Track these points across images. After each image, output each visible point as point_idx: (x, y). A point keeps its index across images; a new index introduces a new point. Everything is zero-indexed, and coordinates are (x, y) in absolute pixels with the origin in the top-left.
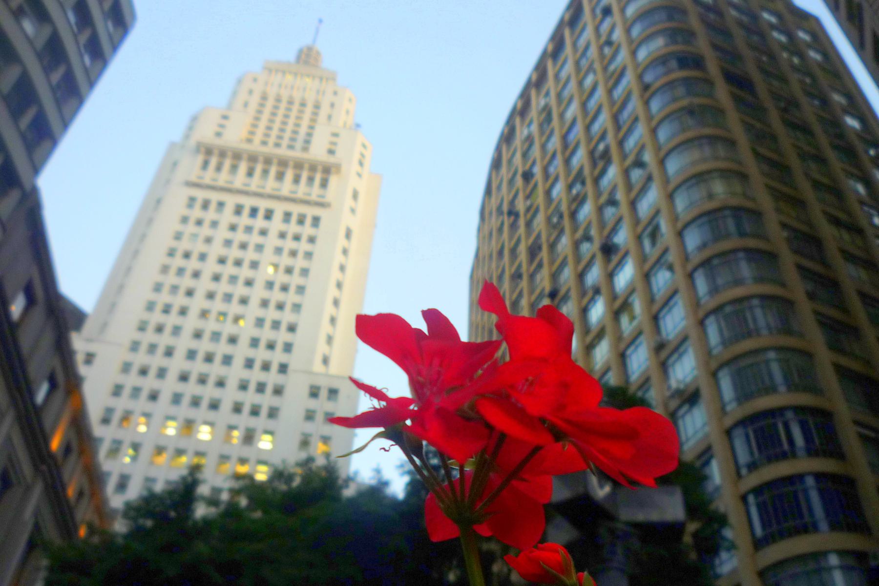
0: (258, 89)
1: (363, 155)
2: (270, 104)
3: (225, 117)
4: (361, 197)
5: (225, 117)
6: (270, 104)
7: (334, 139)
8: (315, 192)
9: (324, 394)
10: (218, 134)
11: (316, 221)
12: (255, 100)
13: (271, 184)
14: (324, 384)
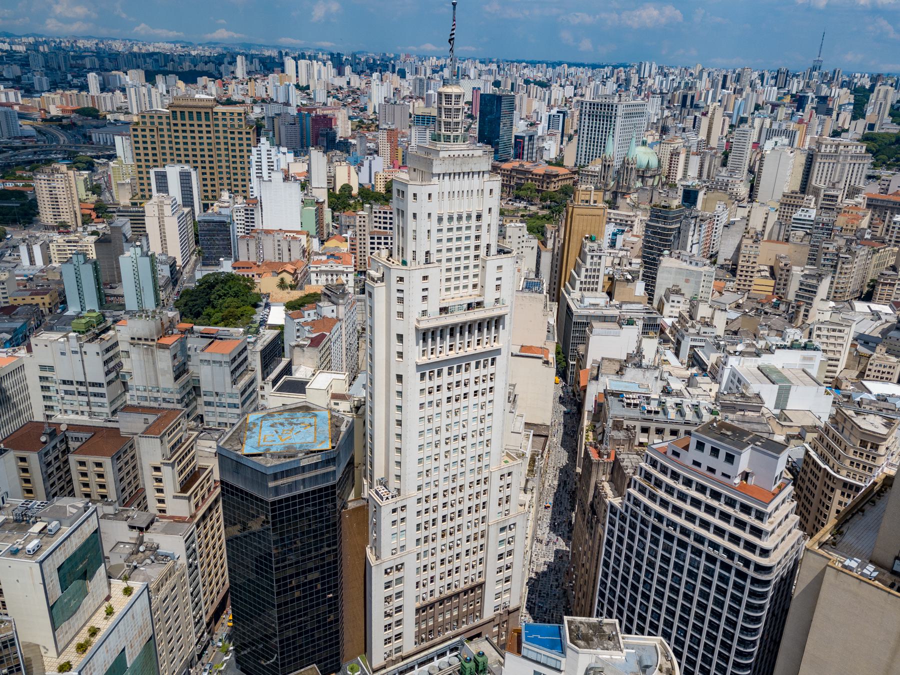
2: (445, 224)
3: (425, 278)
6: (445, 224)
11: (493, 360)
12: (435, 226)
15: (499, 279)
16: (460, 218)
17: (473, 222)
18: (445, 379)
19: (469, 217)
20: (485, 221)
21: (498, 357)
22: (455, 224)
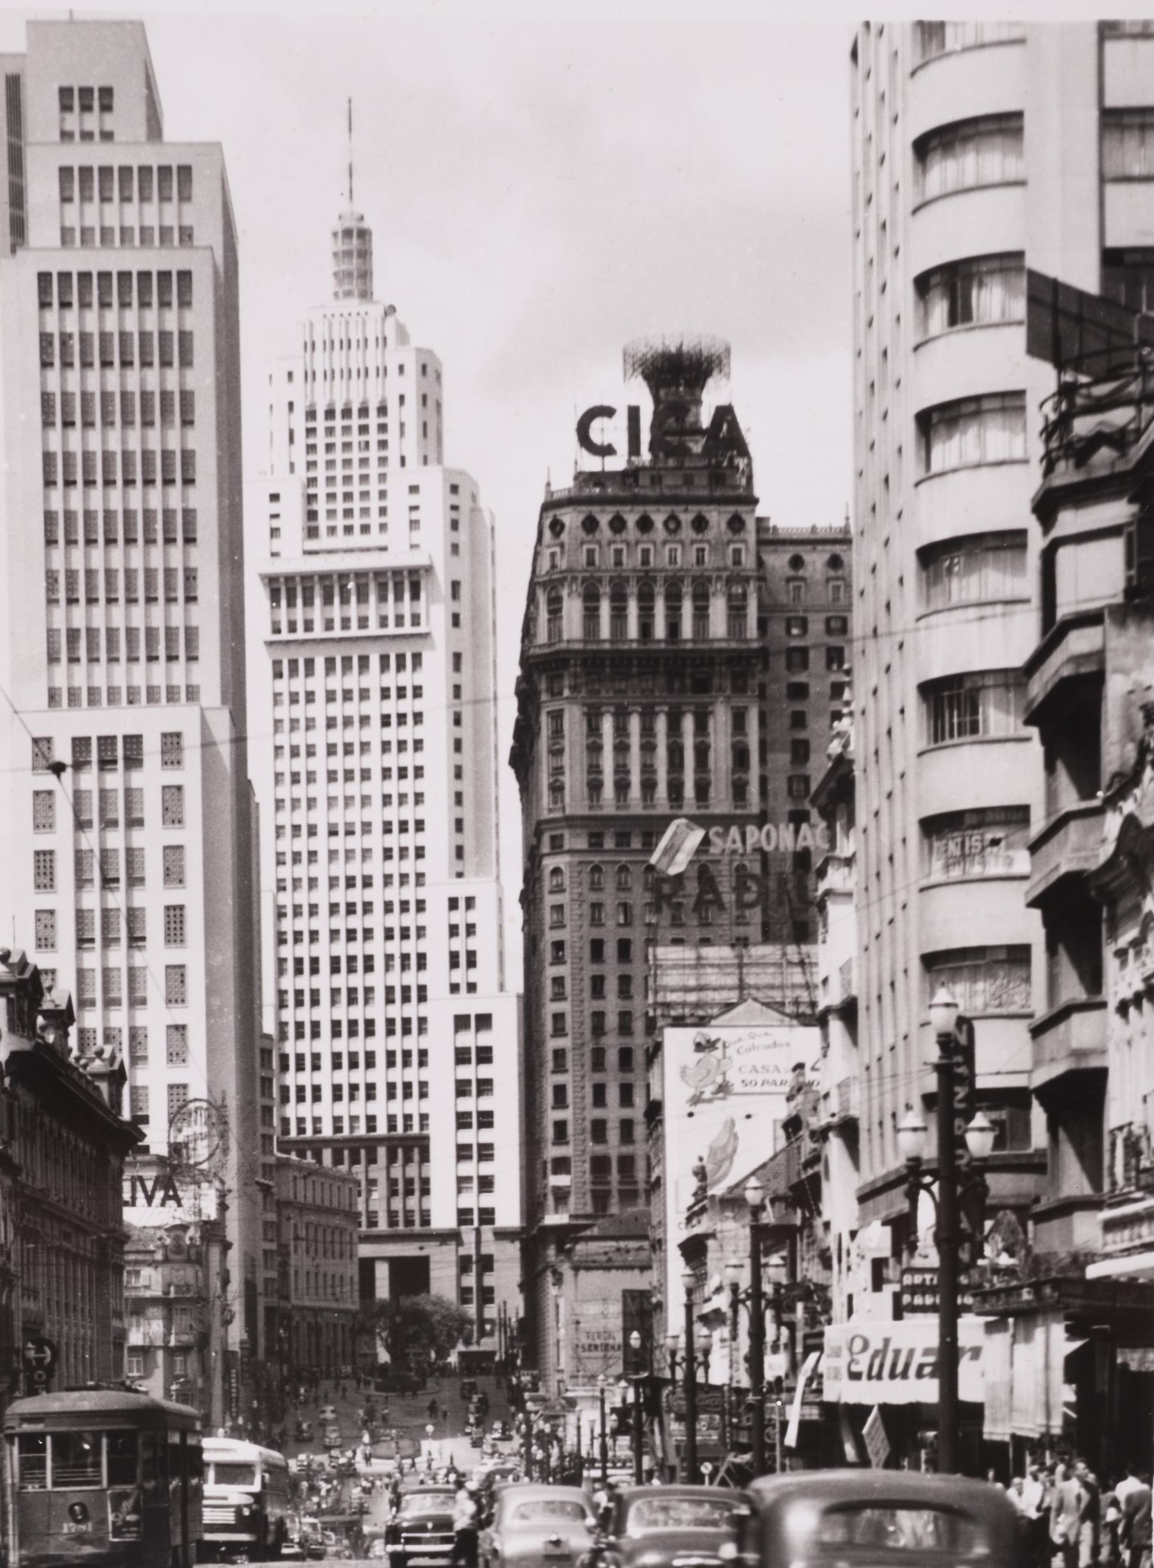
0: (297, 392)
1: (455, 508)
2: (321, 423)
3: (275, 497)
4: (464, 590)
5: (275, 497)
6: (321, 423)
7: (414, 500)
8: (406, 607)
9: (462, 904)
10: (274, 532)
11: (417, 658)
12: (300, 423)
13: (353, 610)
14: (461, 890)
15: (414, 508)
16: (347, 413)
17: (373, 420)
18: (319, 683)
19: (364, 412)
20: (392, 420)
21: (426, 657)
22: (338, 422)
